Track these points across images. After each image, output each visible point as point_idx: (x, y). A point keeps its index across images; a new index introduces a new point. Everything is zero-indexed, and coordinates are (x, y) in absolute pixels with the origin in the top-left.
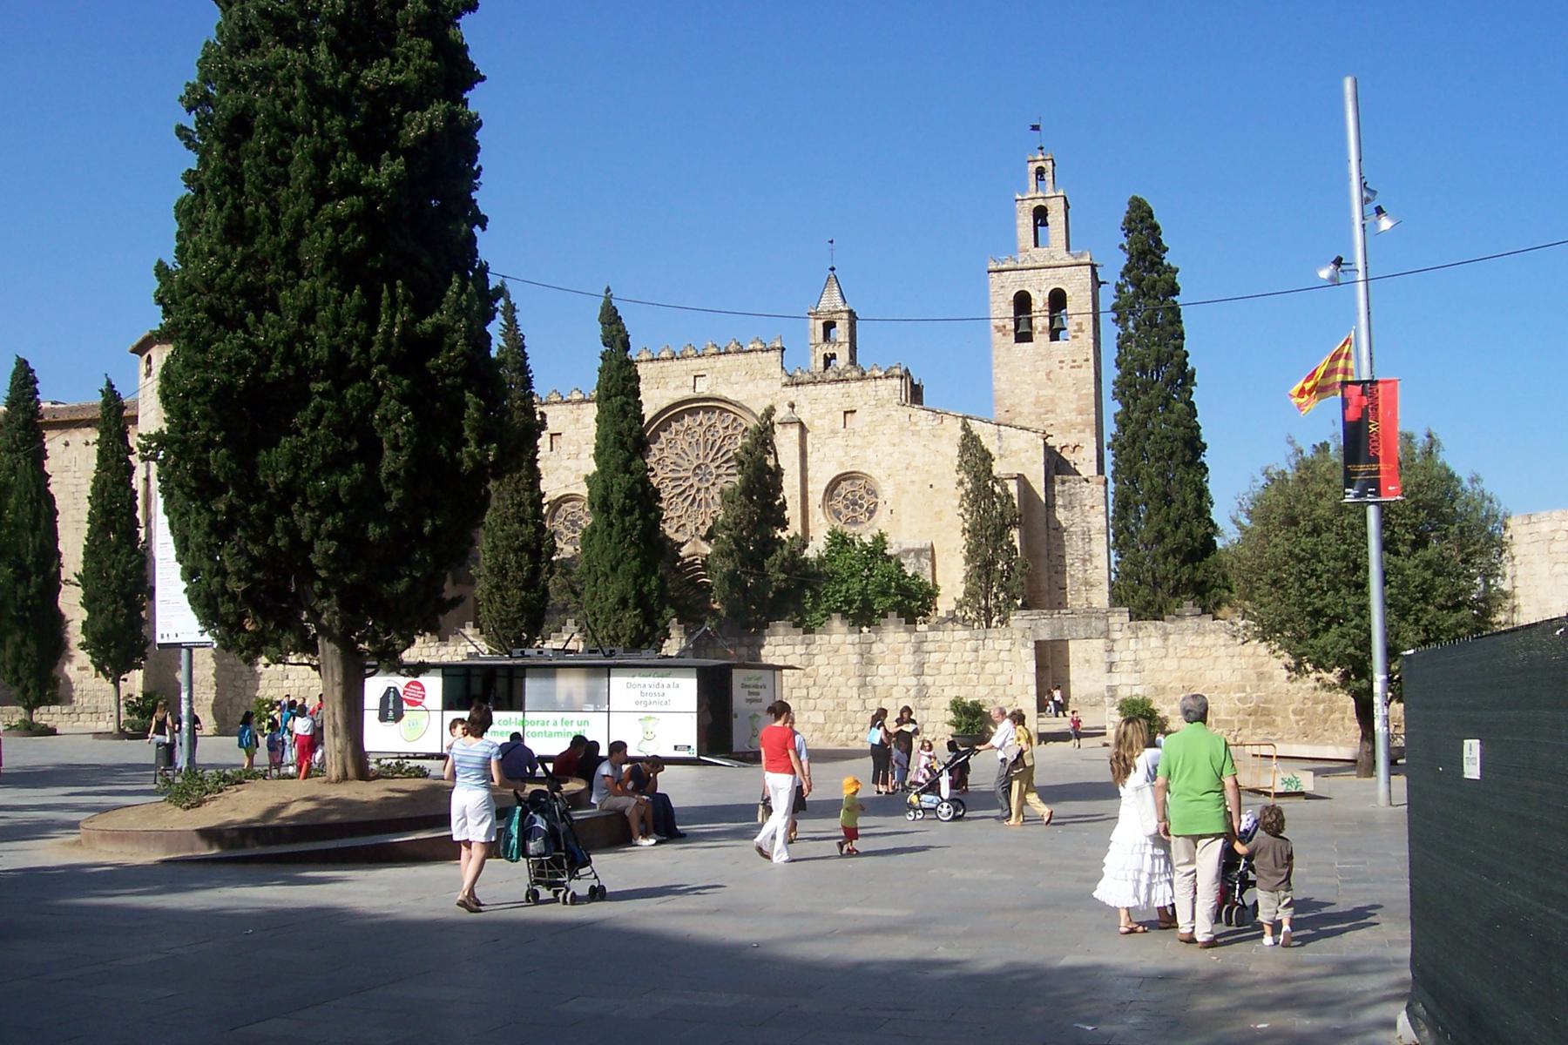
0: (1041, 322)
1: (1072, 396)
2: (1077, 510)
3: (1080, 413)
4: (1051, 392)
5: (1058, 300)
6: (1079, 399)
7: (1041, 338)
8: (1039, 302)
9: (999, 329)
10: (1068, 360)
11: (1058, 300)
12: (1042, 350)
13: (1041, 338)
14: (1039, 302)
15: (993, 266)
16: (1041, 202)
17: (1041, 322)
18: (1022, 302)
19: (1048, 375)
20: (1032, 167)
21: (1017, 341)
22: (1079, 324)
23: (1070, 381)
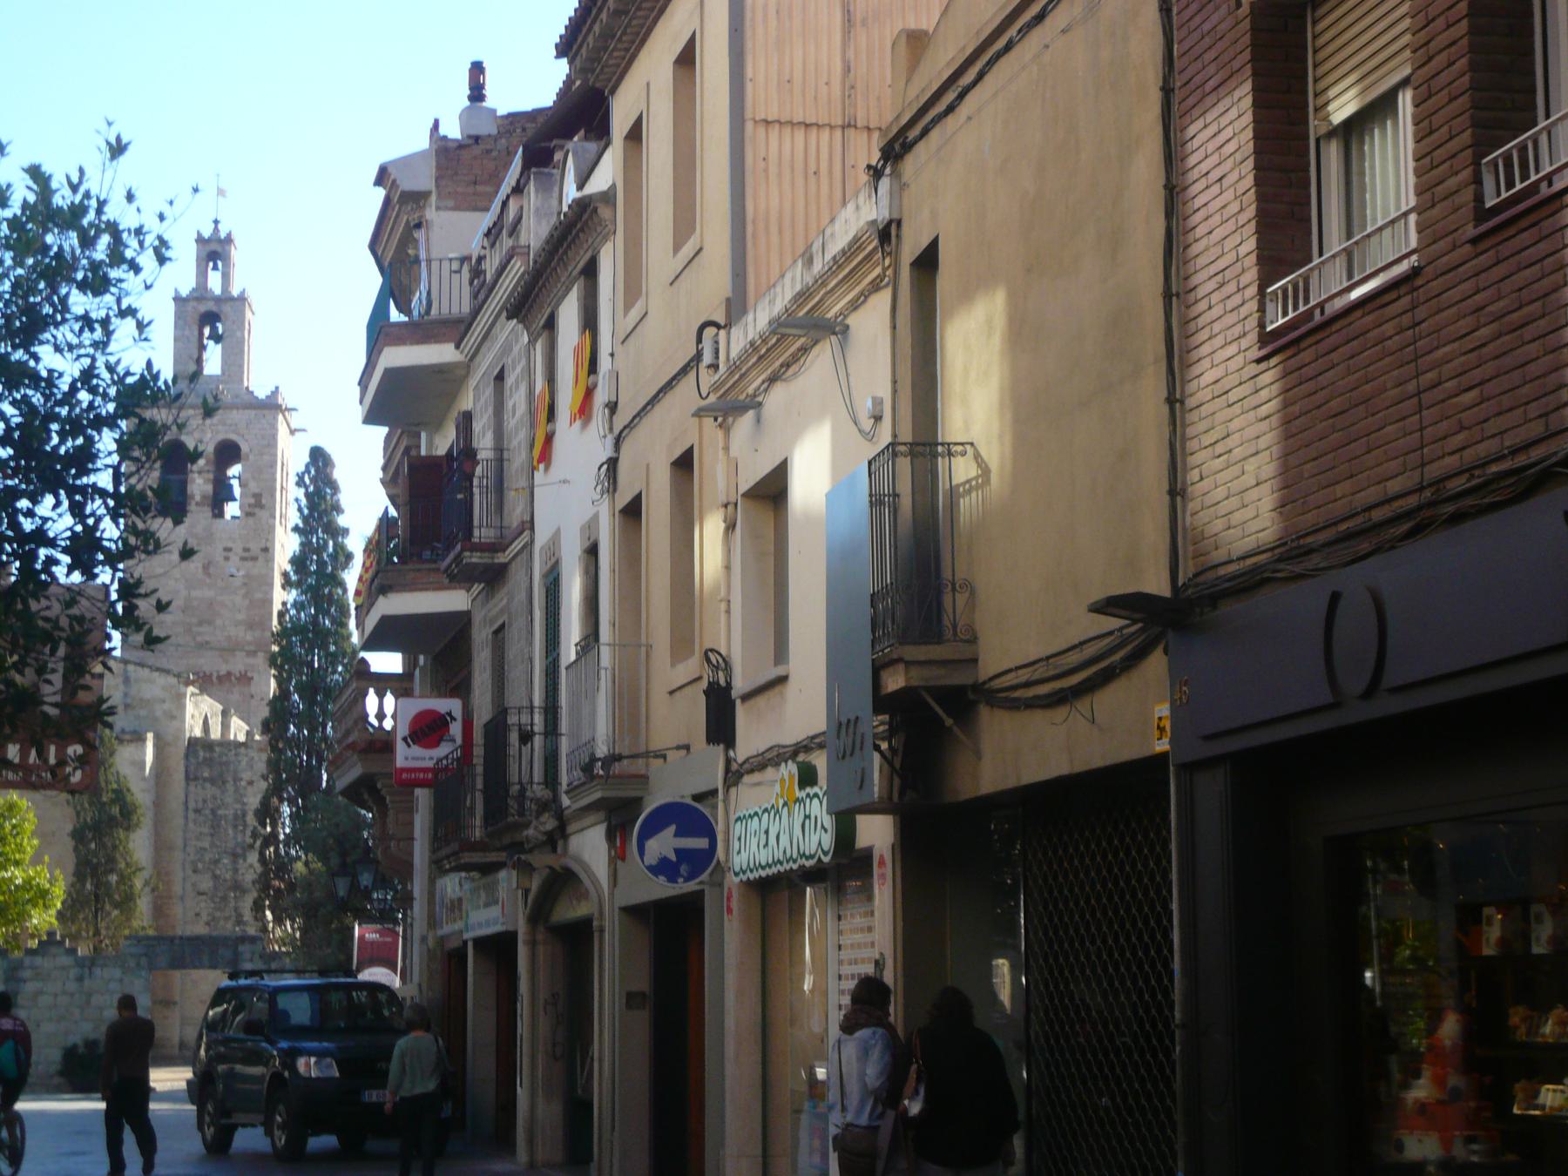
2: (230, 787)
4: (209, 593)
10: (238, 548)
16: (210, 306)
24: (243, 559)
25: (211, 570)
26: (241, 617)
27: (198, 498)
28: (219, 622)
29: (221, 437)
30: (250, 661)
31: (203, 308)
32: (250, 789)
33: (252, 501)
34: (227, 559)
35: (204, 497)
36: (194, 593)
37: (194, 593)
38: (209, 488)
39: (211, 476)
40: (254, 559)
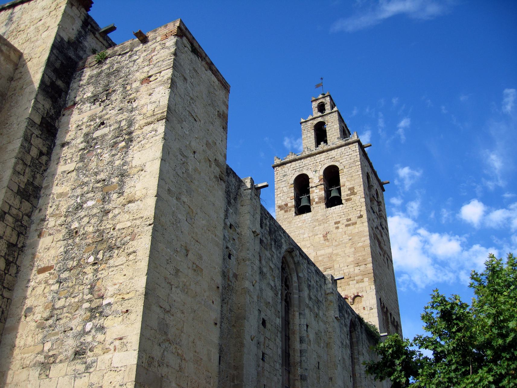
0: (317, 193)
1: (349, 250)
3: (358, 265)
4: (329, 250)
5: (332, 176)
6: (355, 253)
7: (319, 209)
8: (316, 179)
9: (284, 208)
11: (332, 176)
12: (319, 216)
13: (319, 209)
14: (316, 179)
15: (277, 162)
16: (320, 120)
17: (317, 193)
18: (302, 184)
19: (325, 236)
20: (315, 105)
21: (297, 214)
22: (352, 189)
23: (346, 238)
24: (347, 226)
25: (329, 236)
26: (351, 259)
27: (316, 200)
28: (336, 266)
29: (326, 166)
30: (361, 285)
31: (315, 122)
32: (144, 88)
33: (349, 192)
34: (337, 228)
35: (320, 198)
36: (319, 253)
37: (319, 253)
38: (322, 193)
39: (323, 186)
40: (356, 223)
